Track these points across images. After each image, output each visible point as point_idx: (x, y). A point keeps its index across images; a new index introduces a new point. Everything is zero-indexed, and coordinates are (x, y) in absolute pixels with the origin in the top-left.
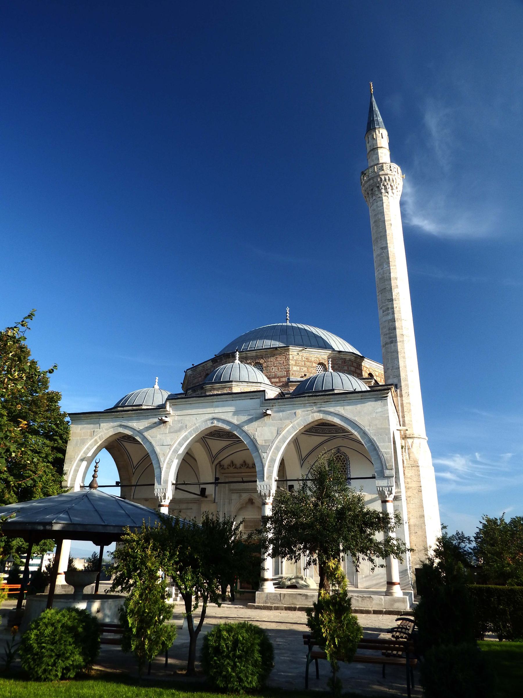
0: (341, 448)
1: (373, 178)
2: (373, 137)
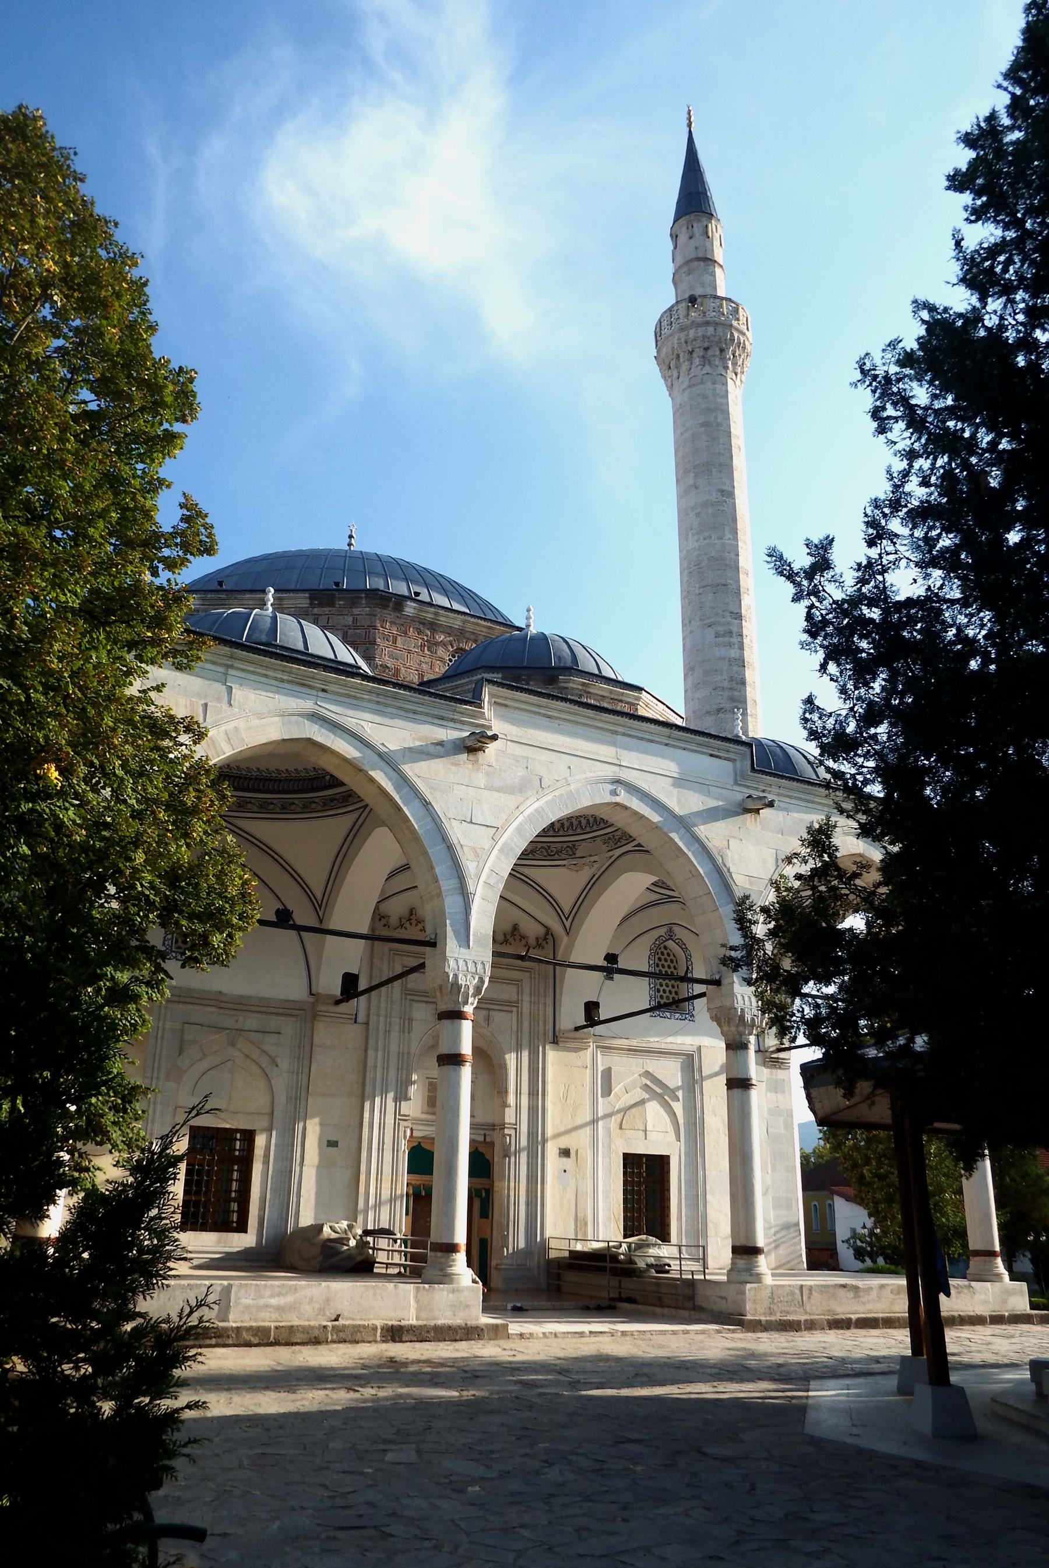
0: (676, 929)
1: (716, 324)
2: (707, 233)
